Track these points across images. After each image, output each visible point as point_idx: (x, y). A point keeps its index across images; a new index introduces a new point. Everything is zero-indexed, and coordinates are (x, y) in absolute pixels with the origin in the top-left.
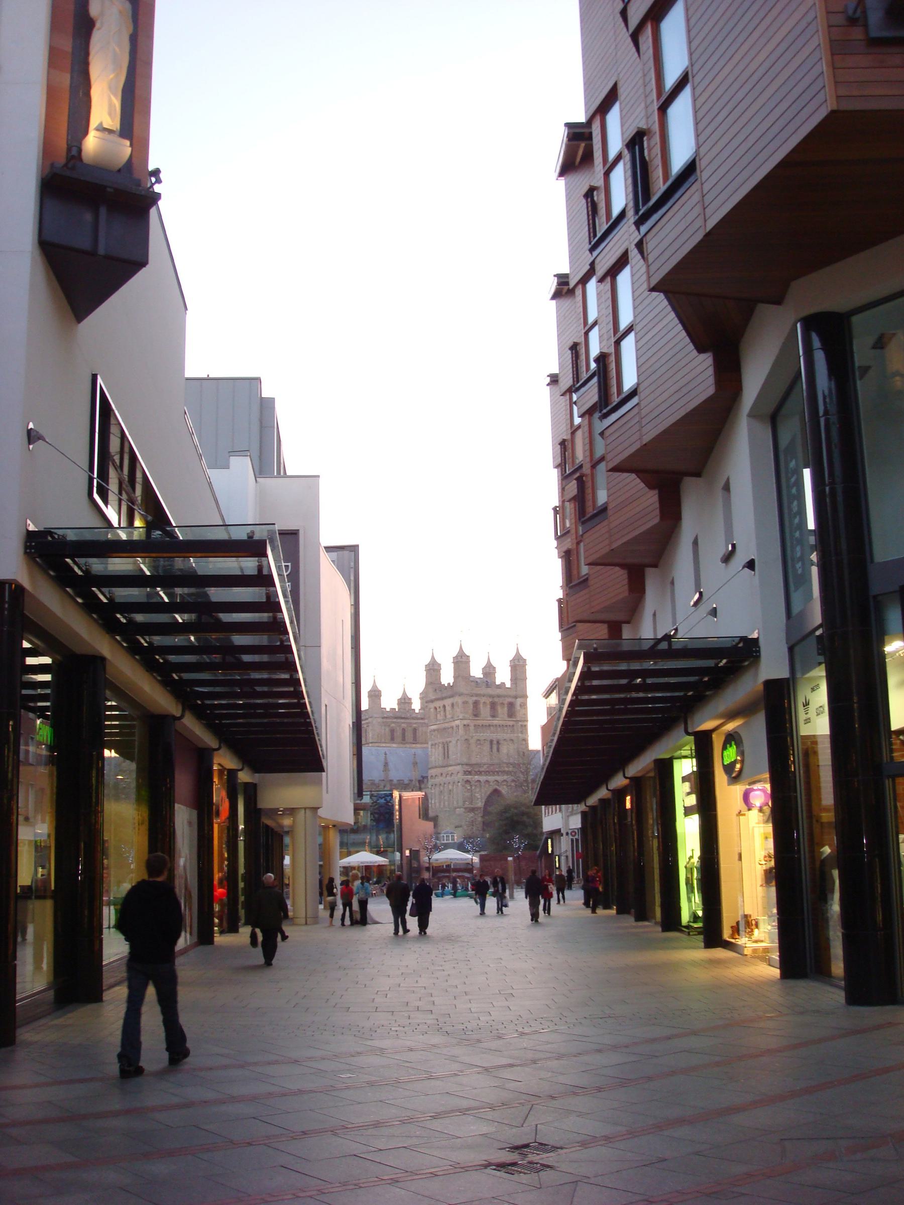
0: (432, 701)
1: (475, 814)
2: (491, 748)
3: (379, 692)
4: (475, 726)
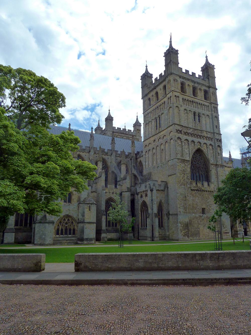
0: (146, 95)
1: (185, 165)
2: (195, 118)
3: (112, 118)
4: (183, 99)
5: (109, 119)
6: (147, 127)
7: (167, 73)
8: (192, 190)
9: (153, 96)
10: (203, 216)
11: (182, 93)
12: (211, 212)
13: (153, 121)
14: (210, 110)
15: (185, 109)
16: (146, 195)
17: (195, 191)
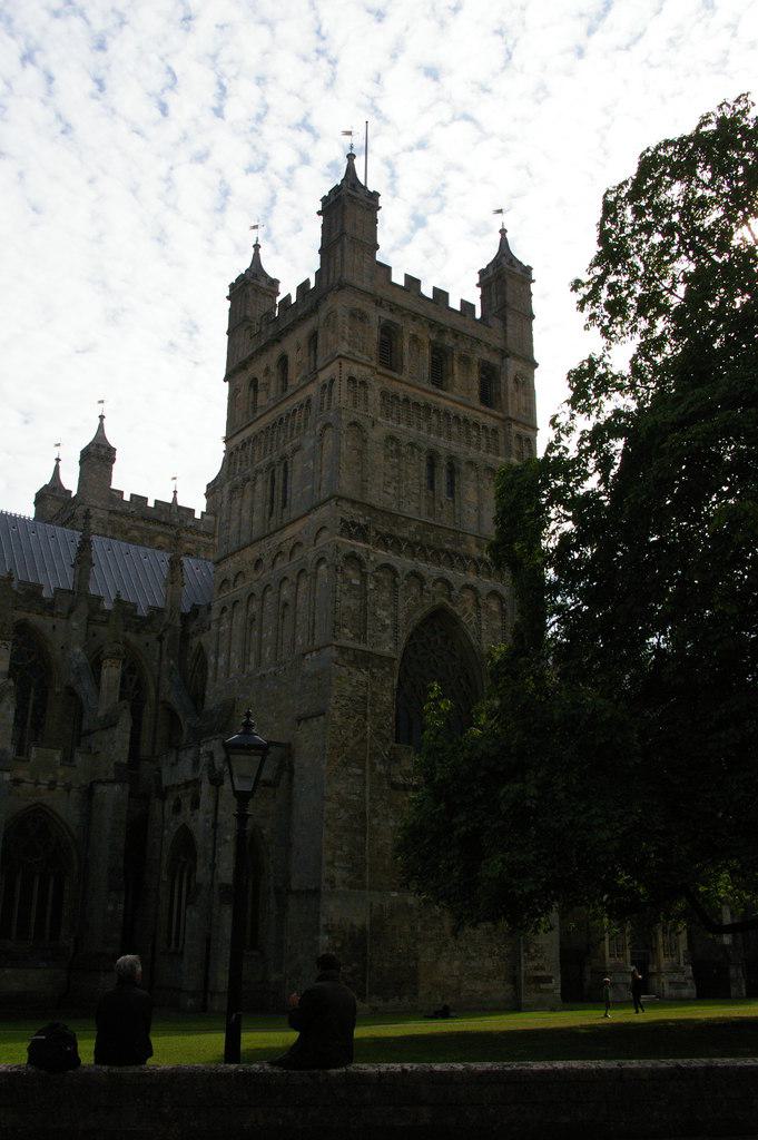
1: (373, 676)
3: (112, 451)
4: (384, 394)
5: (98, 456)
6: (237, 503)
7: (325, 280)
8: (394, 786)
9: (267, 369)
11: (381, 370)
13: (259, 477)
14: (502, 447)
15: (391, 439)
16: (195, 804)
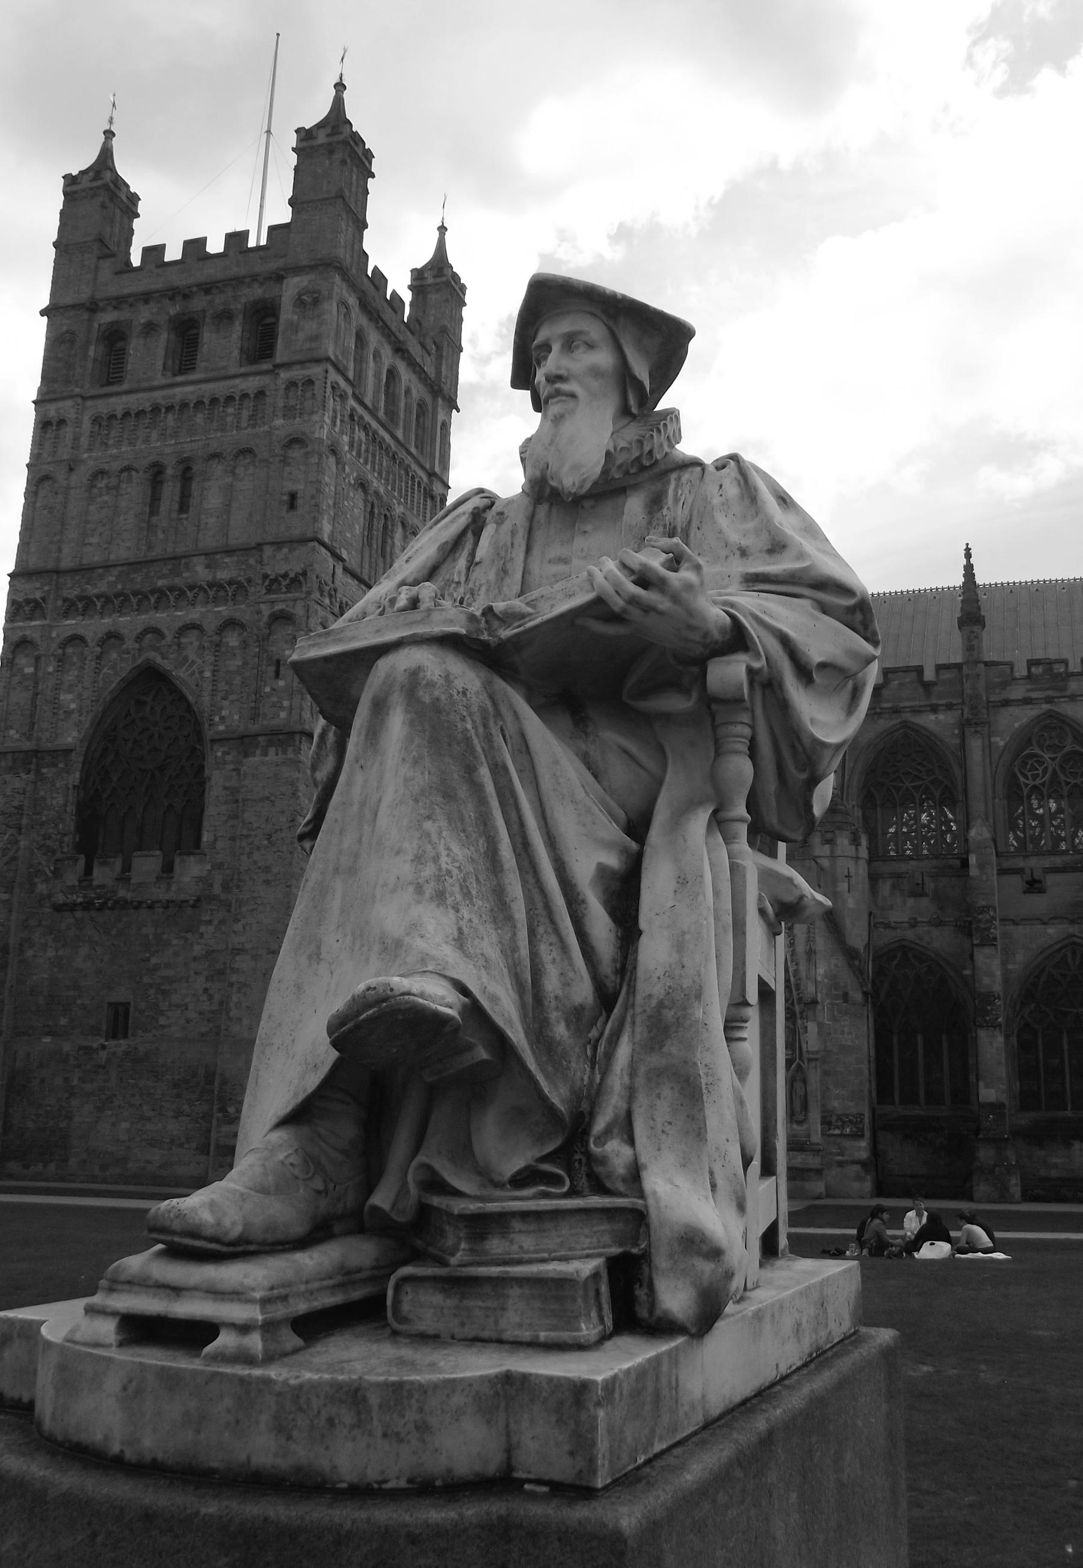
4: (96, 420)
10: (103, 1047)
12: (163, 1027)
17: (79, 914)
